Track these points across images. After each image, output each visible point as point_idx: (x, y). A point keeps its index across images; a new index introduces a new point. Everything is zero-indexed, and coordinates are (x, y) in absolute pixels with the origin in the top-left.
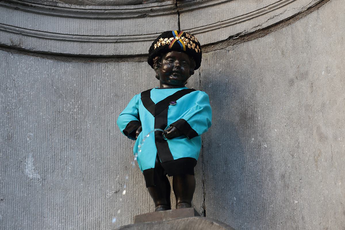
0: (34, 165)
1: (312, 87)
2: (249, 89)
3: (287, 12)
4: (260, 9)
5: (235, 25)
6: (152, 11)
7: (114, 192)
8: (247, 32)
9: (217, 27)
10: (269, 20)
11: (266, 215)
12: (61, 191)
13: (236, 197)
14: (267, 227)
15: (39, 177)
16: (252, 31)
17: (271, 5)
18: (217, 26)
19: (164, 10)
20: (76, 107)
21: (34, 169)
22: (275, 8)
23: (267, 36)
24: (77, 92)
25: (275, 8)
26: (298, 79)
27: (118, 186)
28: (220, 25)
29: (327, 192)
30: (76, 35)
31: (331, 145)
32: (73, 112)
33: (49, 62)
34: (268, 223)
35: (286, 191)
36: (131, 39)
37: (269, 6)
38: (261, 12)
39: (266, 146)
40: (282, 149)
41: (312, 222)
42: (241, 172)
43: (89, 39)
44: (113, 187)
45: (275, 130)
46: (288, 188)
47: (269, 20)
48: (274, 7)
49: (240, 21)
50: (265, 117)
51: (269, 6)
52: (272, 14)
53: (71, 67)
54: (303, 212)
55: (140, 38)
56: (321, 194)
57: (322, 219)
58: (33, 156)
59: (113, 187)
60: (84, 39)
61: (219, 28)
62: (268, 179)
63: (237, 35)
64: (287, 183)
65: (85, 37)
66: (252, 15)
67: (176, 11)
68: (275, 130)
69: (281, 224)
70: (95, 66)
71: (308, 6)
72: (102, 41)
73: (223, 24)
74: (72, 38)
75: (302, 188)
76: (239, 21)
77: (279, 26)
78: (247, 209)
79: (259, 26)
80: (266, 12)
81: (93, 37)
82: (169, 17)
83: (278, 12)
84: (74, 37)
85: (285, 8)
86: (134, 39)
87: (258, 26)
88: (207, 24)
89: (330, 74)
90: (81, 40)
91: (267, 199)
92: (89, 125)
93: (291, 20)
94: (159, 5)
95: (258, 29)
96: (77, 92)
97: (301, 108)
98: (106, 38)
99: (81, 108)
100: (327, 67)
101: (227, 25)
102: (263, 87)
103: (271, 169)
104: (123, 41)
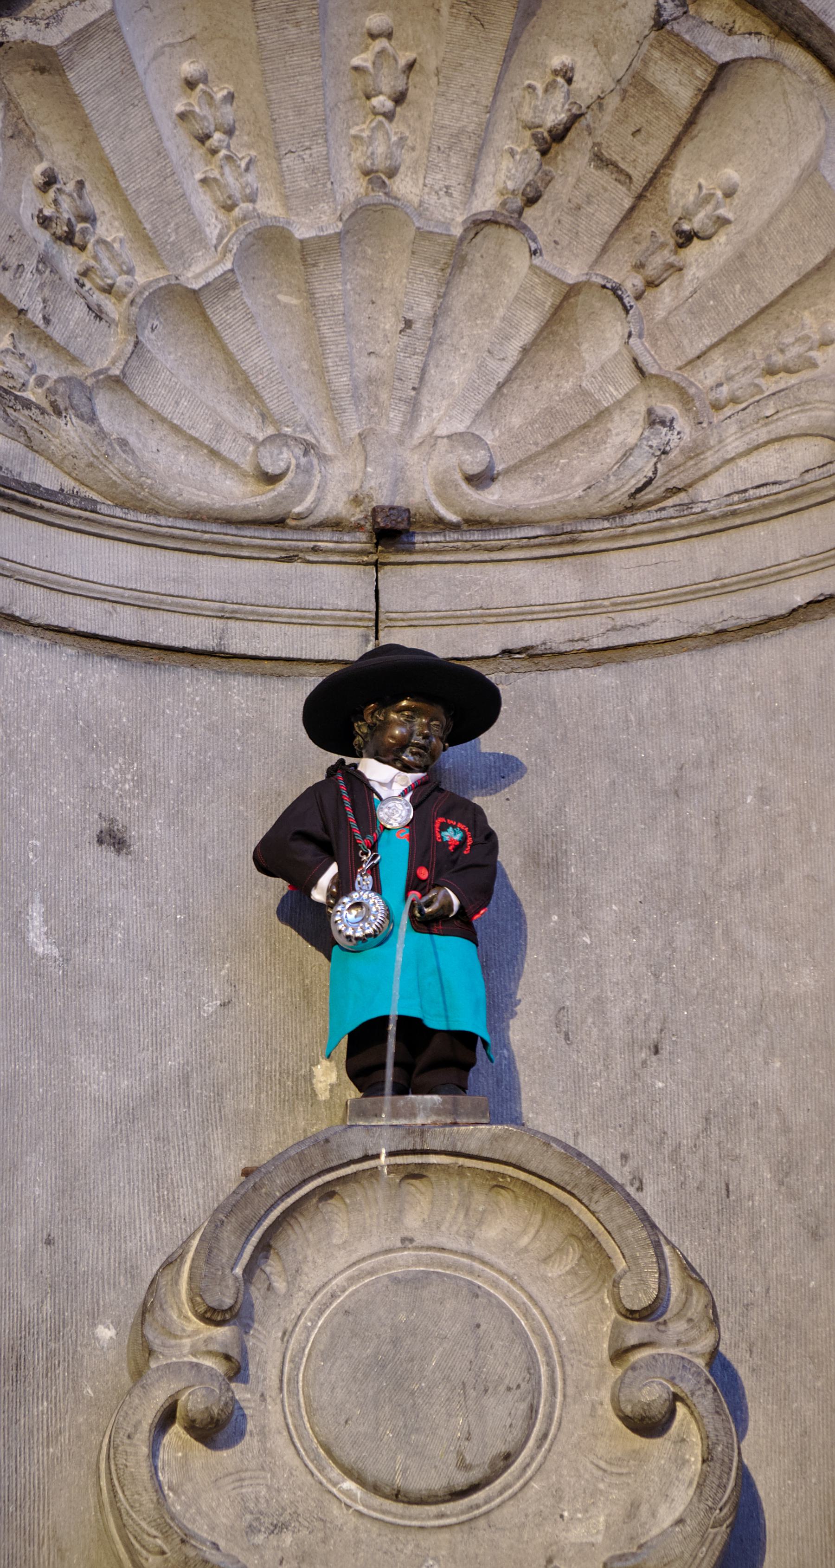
0: (46, 922)
1: (717, 824)
2: (547, 791)
3: (658, 623)
5: (519, 624)
6: (315, 550)
7: (219, 1002)
9: (473, 620)
12: (102, 990)
15: (56, 952)
16: (563, 648)
18: (473, 616)
19: (344, 552)
20: (129, 777)
21: (46, 934)
22: (628, 607)
24: (129, 740)
25: (628, 607)
27: (228, 989)
28: (482, 616)
30: (131, 589)
31: (761, 975)
33: (66, 654)
36: (258, 614)
43: (162, 602)
49: (535, 616)
52: (620, 619)
55: (278, 615)
58: (42, 901)
59: (216, 991)
60: (149, 600)
62: (590, 1020)
65: (152, 596)
66: (567, 610)
67: (373, 558)
71: (718, 627)
72: (190, 611)
73: (490, 616)
74: (122, 597)
76: (530, 617)
78: (534, 1082)
79: (582, 639)
80: (604, 610)
81: (169, 599)
82: (353, 570)
83: (636, 617)
84: (127, 593)
85: (654, 612)
86: (264, 614)
88: (448, 608)
90: (141, 603)
92: (157, 828)
93: (667, 646)
94: (335, 539)
95: (578, 646)
96: (129, 740)
98: (199, 603)
99: (139, 782)
100: (761, 789)
103: (599, 998)
104: (238, 616)
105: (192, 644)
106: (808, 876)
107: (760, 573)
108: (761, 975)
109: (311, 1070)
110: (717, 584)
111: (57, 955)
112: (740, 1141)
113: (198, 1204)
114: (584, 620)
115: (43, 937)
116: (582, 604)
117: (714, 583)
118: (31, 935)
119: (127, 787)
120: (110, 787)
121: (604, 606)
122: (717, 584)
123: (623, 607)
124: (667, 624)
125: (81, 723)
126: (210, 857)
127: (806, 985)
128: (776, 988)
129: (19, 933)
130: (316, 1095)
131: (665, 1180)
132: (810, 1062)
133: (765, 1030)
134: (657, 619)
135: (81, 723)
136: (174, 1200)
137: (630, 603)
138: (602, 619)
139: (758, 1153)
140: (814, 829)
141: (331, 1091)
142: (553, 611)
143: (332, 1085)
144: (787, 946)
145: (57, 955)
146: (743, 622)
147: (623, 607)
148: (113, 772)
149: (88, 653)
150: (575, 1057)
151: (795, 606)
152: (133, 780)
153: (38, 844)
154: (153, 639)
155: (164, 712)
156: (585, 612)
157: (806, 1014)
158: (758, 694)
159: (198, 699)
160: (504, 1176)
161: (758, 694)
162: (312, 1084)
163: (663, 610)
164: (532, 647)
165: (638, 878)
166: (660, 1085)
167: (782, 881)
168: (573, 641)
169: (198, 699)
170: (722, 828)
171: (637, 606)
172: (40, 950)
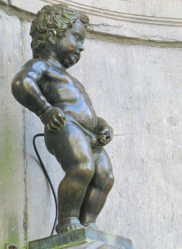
1: (149, 129)
4: (95, 8)
10: (100, 24)
17: (108, 10)
23: (94, 41)
31: (172, 205)
35: (111, 231)
37: (106, 10)
38: (96, 11)
46: (114, 228)
47: (100, 24)
48: (110, 14)
51: (106, 10)
64: (113, 223)
71: (152, 39)
75: (129, 235)
80: (100, 14)
83: (112, 22)
89: (174, 127)
97: (132, 145)
100: (171, 118)
107: (176, 20)
108: (172, 205)
110: (153, 19)
116: (92, 9)
117: (152, 18)
121: (101, 13)
122: (153, 19)
123: (108, 16)
124: (126, 30)
134: (122, 26)
137: (112, 15)
138: (99, 18)
142: (79, 7)
147: (108, 16)
156: (92, 13)
158: (169, 74)
171: (114, 17)
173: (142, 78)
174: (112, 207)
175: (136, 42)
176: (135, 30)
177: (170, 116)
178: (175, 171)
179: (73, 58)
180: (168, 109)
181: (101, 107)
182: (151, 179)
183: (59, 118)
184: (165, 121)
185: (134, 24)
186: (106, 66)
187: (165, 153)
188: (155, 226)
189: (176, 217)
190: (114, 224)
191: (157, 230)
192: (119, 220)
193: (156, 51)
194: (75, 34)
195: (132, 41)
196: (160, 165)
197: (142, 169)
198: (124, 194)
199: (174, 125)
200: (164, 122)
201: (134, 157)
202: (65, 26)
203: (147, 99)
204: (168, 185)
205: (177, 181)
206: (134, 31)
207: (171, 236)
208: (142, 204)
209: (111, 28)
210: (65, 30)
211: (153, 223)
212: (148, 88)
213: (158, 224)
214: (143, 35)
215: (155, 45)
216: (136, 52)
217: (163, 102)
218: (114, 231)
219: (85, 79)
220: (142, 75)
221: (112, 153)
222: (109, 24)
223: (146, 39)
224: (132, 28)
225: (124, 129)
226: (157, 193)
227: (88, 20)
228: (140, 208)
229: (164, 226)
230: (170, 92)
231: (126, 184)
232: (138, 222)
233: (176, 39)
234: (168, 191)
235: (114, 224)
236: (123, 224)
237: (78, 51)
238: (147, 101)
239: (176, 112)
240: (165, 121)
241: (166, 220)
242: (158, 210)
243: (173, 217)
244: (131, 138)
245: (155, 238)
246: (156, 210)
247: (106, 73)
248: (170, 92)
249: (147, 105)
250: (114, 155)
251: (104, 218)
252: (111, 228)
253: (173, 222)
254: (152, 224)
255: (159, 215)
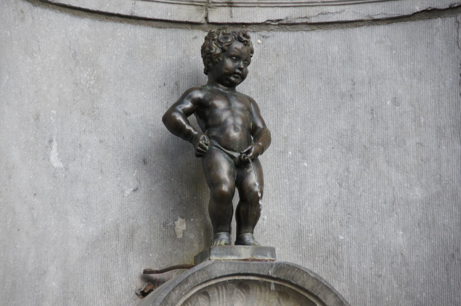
0: (58, 151)
1: (372, 113)
3: (344, 13)
7: (132, 189)
8: (290, 21)
9: (253, 5)
11: (303, 244)
13: (267, 216)
14: (303, 257)
15: (61, 165)
20: (93, 78)
23: (314, 33)
24: (93, 59)
26: (352, 98)
29: (384, 237)
32: (89, 84)
34: (304, 253)
39: (306, 165)
40: (327, 174)
41: (361, 264)
42: (274, 188)
44: (131, 184)
45: (319, 149)
46: (332, 219)
50: (306, 131)
53: (86, 25)
54: (350, 251)
56: (375, 237)
57: (373, 263)
58: (57, 140)
59: (131, 184)
61: (255, 7)
62: (307, 204)
63: (278, 20)
68: (319, 149)
69: (320, 257)
70: (109, 26)
71: (376, 17)
73: (261, 3)
77: (330, 26)
79: (306, 17)
80: (318, 4)
83: (332, 9)
85: (343, 7)
87: (304, 18)
89: (398, 107)
91: (304, 226)
95: (305, 21)
96: (93, 59)
97: (354, 134)
100: (395, 98)
101: (266, 5)
102: (306, 94)
105: (122, 12)
106: (418, 143)
109: (174, 223)
111: (62, 167)
112: (382, 268)
113: (122, 289)
114: (307, 8)
115: (57, 158)
118: (52, 157)
119: (92, 83)
120: (84, 83)
125: (72, 52)
126: (129, 118)
127: (416, 196)
128: (401, 196)
129: (47, 157)
130: (176, 235)
131: (344, 284)
132: (418, 233)
133: (396, 215)
134: (344, 11)
135: (72, 52)
136: (111, 287)
138: (317, 8)
139: (391, 275)
140: (422, 121)
141: (183, 233)
143: (184, 231)
144: (407, 176)
145: (62, 167)
146: (388, 16)
148: (86, 75)
149: (74, 15)
150: (299, 221)
151: (416, 11)
152: (94, 79)
153: (55, 112)
154: (104, 10)
155: (108, 45)
157: (417, 210)
158: (394, 52)
159: (123, 39)
160: (284, 286)
161: (394, 52)
162: (174, 230)
163: (347, 7)
164: (281, 20)
165: (331, 136)
166: (342, 238)
167: (405, 144)
168: (302, 18)
169: (123, 39)
170: (375, 115)
172: (55, 165)
173: (367, 61)
174: (331, 198)
175: (360, 24)
176: (358, 12)
177: (394, 96)
178: (397, 153)
179: (233, 79)
180: (392, 89)
181: (321, 99)
182: (373, 165)
183: (201, 146)
184: (388, 103)
185: (357, 5)
186: (327, 56)
187: (388, 136)
188: (376, 212)
189: (396, 200)
190: (332, 215)
191: (377, 216)
192: (339, 210)
193: (381, 30)
194: (231, 57)
195: (357, 23)
196: (383, 149)
197: (364, 155)
198: (344, 184)
199: (398, 106)
200: (388, 103)
201: (356, 145)
202: (218, 51)
203: (371, 82)
204: (390, 169)
205: (399, 163)
206: (357, 13)
207: (391, 220)
208: (363, 191)
209: (332, 15)
210: (218, 55)
211: (374, 209)
212: (373, 71)
213: (379, 211)
214: (367, 15)
215: (380, 23)
216: (361, 35)
217: (388, 83)
218: (333, 222)
219: (303, 74)
220: (367, 58)
221: (333, 144)
222: (330, 11)
223: (370, 19)
224: (355, 10)
225: (346, 118)
226: (379, 177)
227: (248, 37)
228: (361, 195)
229: (385, 211)
230: (395, 71)
231: (346, 174)
232: (358, 210)
233: (400, 13)
234: (390, 175)
235: (332, 215)
236: (343, 214)
237: (238, 71)
238: (371, 85)
239: (400, 91)
240: (388, 103)
241: (387, 204)
242: (379, 195)
243: (394, 201)
244: (353, 126)
245: (376, 223)
246: (377, 195)
247: (327, 63)
248: (395, 71)
249: (372, 88)
250: (335, 146)
251: (322, 210)
252: (330, 219)
253: (394, 206)
254: (373, 211)
255: (380, 201)
